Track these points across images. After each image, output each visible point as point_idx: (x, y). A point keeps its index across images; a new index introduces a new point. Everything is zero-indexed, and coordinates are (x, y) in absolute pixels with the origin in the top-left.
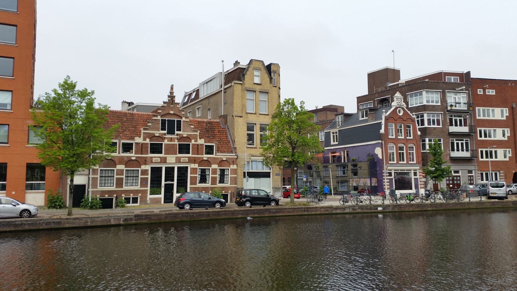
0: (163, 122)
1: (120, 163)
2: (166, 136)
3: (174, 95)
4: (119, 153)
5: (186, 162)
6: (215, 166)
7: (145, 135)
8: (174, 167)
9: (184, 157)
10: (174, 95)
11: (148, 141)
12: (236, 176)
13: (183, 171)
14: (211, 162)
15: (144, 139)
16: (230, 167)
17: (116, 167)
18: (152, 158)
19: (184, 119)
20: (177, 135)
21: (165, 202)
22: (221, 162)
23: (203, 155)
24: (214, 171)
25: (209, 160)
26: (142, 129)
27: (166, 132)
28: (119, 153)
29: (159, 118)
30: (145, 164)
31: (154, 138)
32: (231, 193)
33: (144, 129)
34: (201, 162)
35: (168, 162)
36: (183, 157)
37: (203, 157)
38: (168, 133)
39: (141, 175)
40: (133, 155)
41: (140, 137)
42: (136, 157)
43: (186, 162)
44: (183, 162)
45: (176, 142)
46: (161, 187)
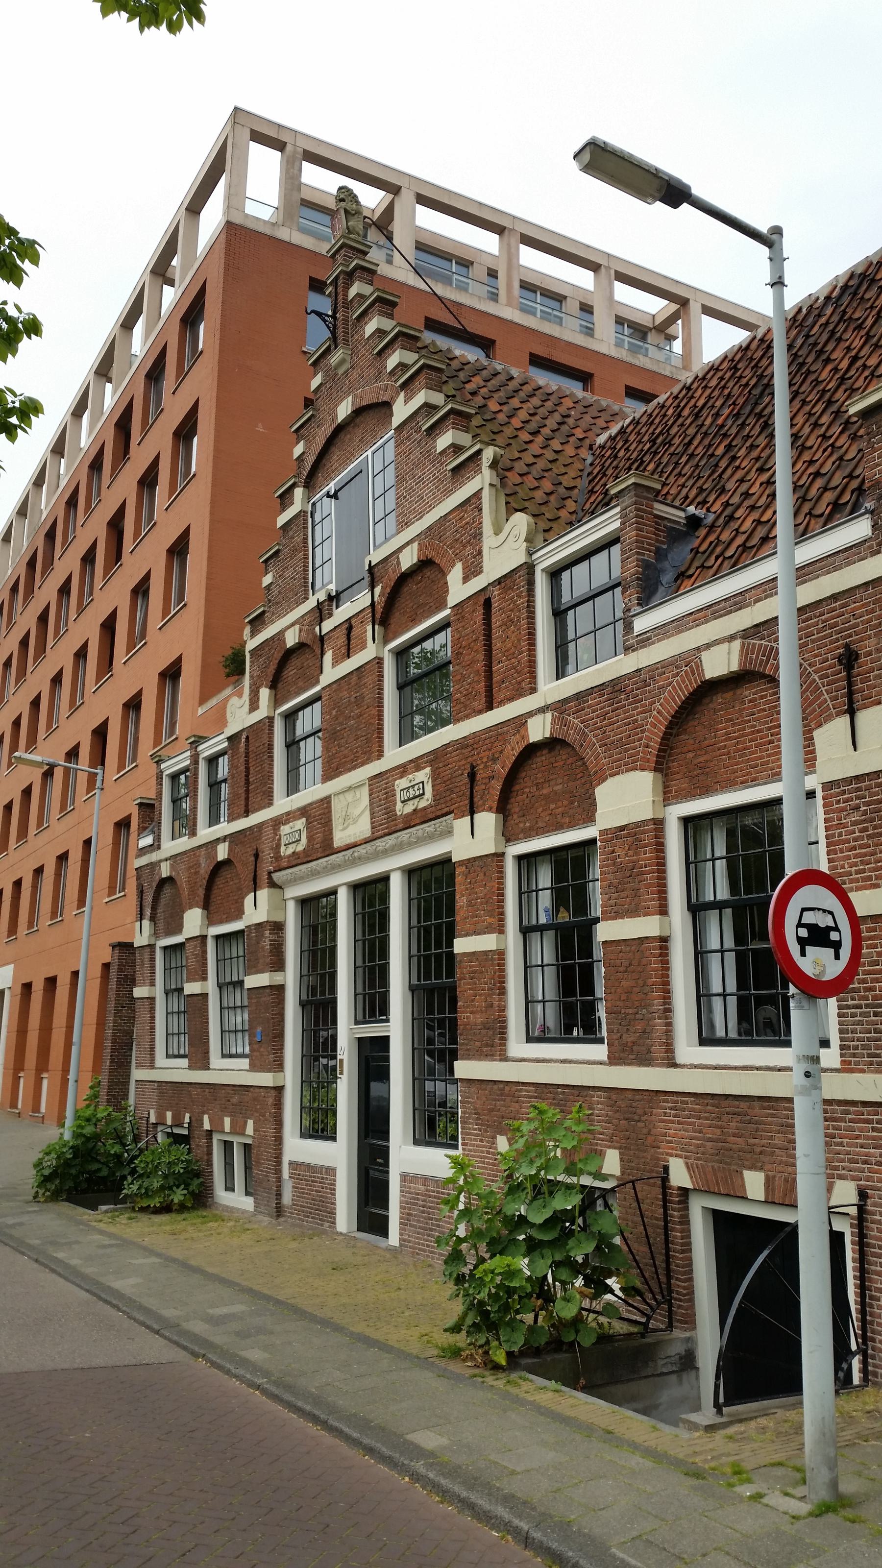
37: (520, 722)
44: (409, 822)
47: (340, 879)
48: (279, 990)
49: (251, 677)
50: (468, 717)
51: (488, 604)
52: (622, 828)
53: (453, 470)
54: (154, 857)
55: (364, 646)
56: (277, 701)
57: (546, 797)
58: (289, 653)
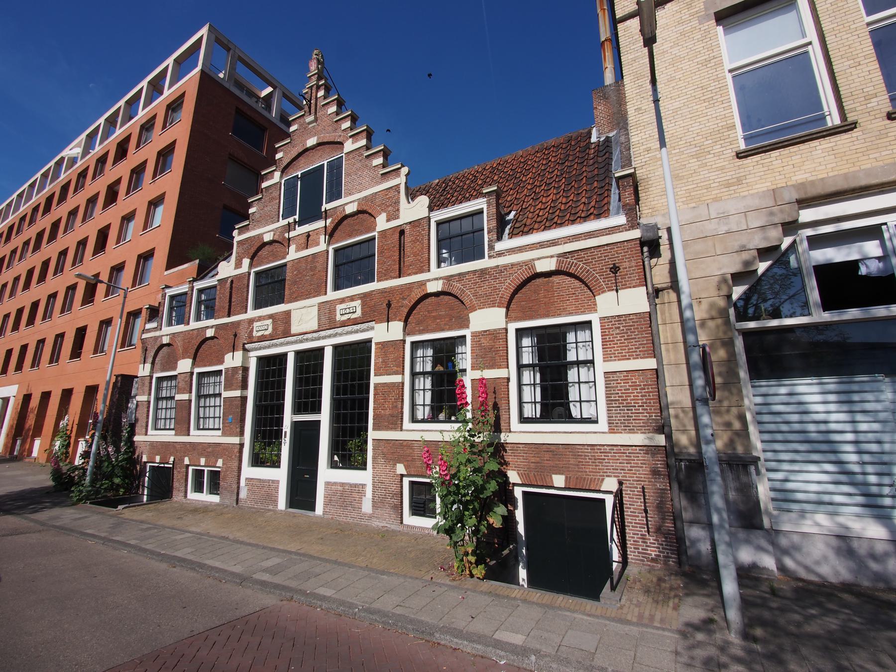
5: (355, 322)
9: (348, 300)
12: (651, 363)
14: (468, 297)
15: (238, 265)
16: (593, 308)
18: (251, 321)
24: (491, 348)
25: (457, 287)
29: (277, 175)
31: (264, 252)
34: (414, 308)
35: (293, 331)
37: (423, 284)
38: (301, 223)
43: (355, 322)
44: (344, 324)
46: (279, 434)
47: (290, 349)
48: (244, 399)
50: (386, 279)
51: (402, 233)
52: (485, 331)
53: (382, 174)
54: (157, 334)
55: (318, 244)
56: (251, 266)
57: (435, 318)
58: (265, 244)
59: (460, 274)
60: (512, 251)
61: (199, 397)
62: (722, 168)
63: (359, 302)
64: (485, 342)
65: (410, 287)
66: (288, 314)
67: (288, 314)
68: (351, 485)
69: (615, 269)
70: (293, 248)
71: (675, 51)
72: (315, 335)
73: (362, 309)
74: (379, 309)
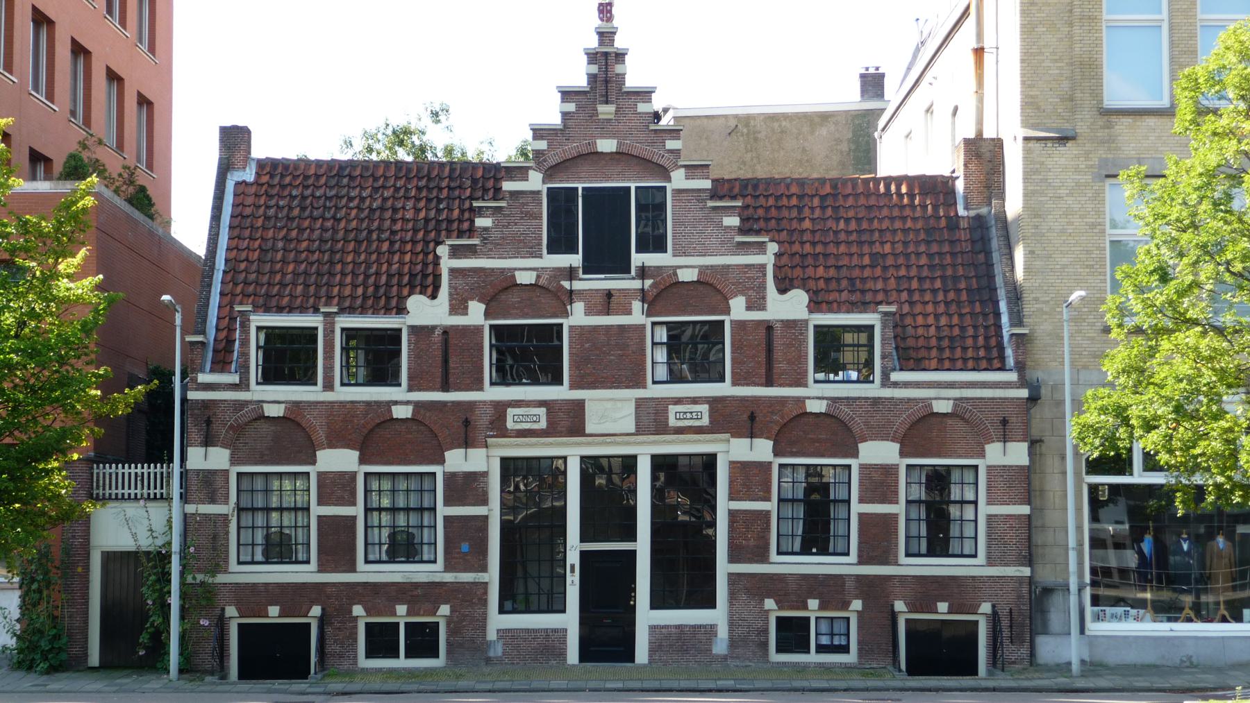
0: (561, 202)
1: (336, 441)
2: (577, 285)
3: (619, 43)
4: (329, 386)
5: (699, 430)
6: (879, 452)
7: (460, 282)
8: (630, 463)
10: (619, 43)
11: (476, 314)
12: (1025, 510)
13: (686, 480)
14: (858, 426)
15: (458, 307)
17: (855, 454)
18: (500, 408)
19: (679, 179)
20: (643, 272)
21: (584, 656)
22: (919, 430)
23: (800, 382)
24: (879, 483)
26: (443, 251)
27: (576, 260)
28: (329, 386)
30: (467, 442)
31: (513, 298)
32: (994, 618)
33: (456, 252)
34: (791, 429)
35: (589, 429)
36: (678, 401)
37: (800, 401)
38: (590, 266)
39: (447, 502)
40: (400, 398)
41: (434, 296)
42: (418, 406)
43: (699, 430)
44: (680, 431)
45: (637, 316)
49: (450, 286)
50: (748, 385)
55: (629, 313)
59: (847, 398)
60: (906, 385)
61: (367, 510)
62: (1092, 339)
63: (706, 406)
64: (876, 476)
65: (783, 401)
66: (579, 406)
67: (579, 406)
68: (694, 627)
69: (1004, 422)
70: (578, 307)
71: (1070, 200)
72: (627, 438)
73: (710, 416)
74: (733, 418)
